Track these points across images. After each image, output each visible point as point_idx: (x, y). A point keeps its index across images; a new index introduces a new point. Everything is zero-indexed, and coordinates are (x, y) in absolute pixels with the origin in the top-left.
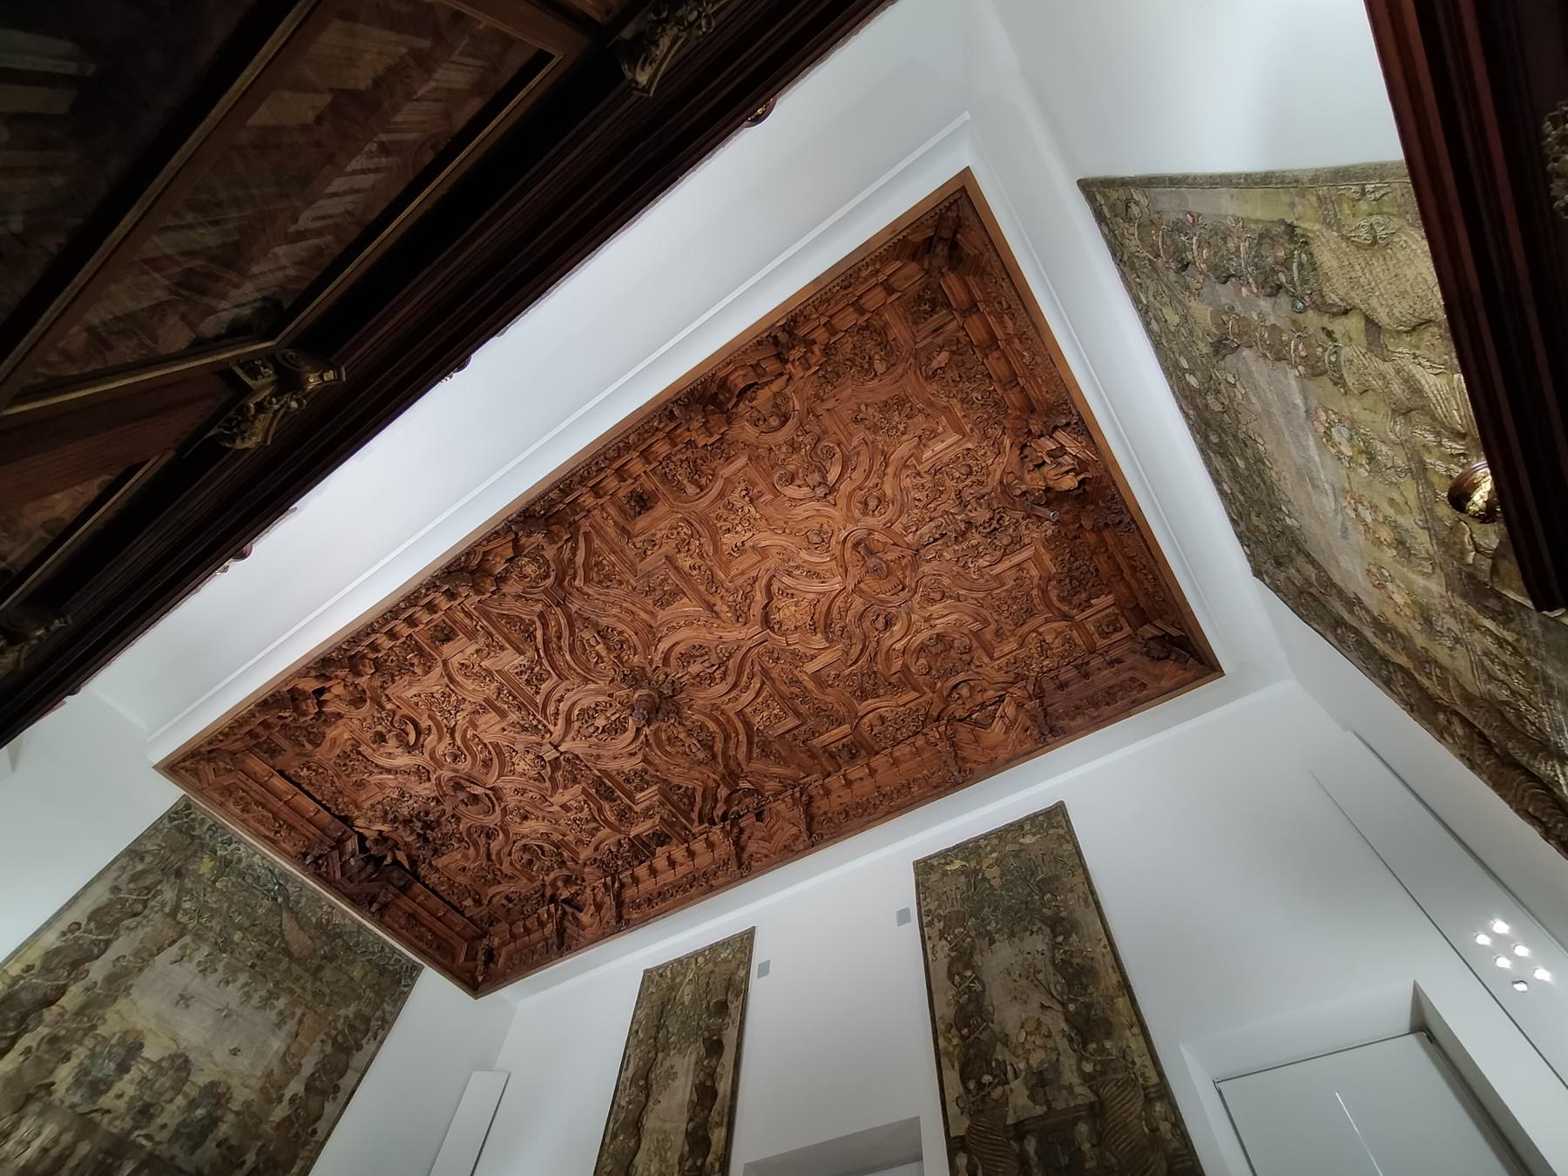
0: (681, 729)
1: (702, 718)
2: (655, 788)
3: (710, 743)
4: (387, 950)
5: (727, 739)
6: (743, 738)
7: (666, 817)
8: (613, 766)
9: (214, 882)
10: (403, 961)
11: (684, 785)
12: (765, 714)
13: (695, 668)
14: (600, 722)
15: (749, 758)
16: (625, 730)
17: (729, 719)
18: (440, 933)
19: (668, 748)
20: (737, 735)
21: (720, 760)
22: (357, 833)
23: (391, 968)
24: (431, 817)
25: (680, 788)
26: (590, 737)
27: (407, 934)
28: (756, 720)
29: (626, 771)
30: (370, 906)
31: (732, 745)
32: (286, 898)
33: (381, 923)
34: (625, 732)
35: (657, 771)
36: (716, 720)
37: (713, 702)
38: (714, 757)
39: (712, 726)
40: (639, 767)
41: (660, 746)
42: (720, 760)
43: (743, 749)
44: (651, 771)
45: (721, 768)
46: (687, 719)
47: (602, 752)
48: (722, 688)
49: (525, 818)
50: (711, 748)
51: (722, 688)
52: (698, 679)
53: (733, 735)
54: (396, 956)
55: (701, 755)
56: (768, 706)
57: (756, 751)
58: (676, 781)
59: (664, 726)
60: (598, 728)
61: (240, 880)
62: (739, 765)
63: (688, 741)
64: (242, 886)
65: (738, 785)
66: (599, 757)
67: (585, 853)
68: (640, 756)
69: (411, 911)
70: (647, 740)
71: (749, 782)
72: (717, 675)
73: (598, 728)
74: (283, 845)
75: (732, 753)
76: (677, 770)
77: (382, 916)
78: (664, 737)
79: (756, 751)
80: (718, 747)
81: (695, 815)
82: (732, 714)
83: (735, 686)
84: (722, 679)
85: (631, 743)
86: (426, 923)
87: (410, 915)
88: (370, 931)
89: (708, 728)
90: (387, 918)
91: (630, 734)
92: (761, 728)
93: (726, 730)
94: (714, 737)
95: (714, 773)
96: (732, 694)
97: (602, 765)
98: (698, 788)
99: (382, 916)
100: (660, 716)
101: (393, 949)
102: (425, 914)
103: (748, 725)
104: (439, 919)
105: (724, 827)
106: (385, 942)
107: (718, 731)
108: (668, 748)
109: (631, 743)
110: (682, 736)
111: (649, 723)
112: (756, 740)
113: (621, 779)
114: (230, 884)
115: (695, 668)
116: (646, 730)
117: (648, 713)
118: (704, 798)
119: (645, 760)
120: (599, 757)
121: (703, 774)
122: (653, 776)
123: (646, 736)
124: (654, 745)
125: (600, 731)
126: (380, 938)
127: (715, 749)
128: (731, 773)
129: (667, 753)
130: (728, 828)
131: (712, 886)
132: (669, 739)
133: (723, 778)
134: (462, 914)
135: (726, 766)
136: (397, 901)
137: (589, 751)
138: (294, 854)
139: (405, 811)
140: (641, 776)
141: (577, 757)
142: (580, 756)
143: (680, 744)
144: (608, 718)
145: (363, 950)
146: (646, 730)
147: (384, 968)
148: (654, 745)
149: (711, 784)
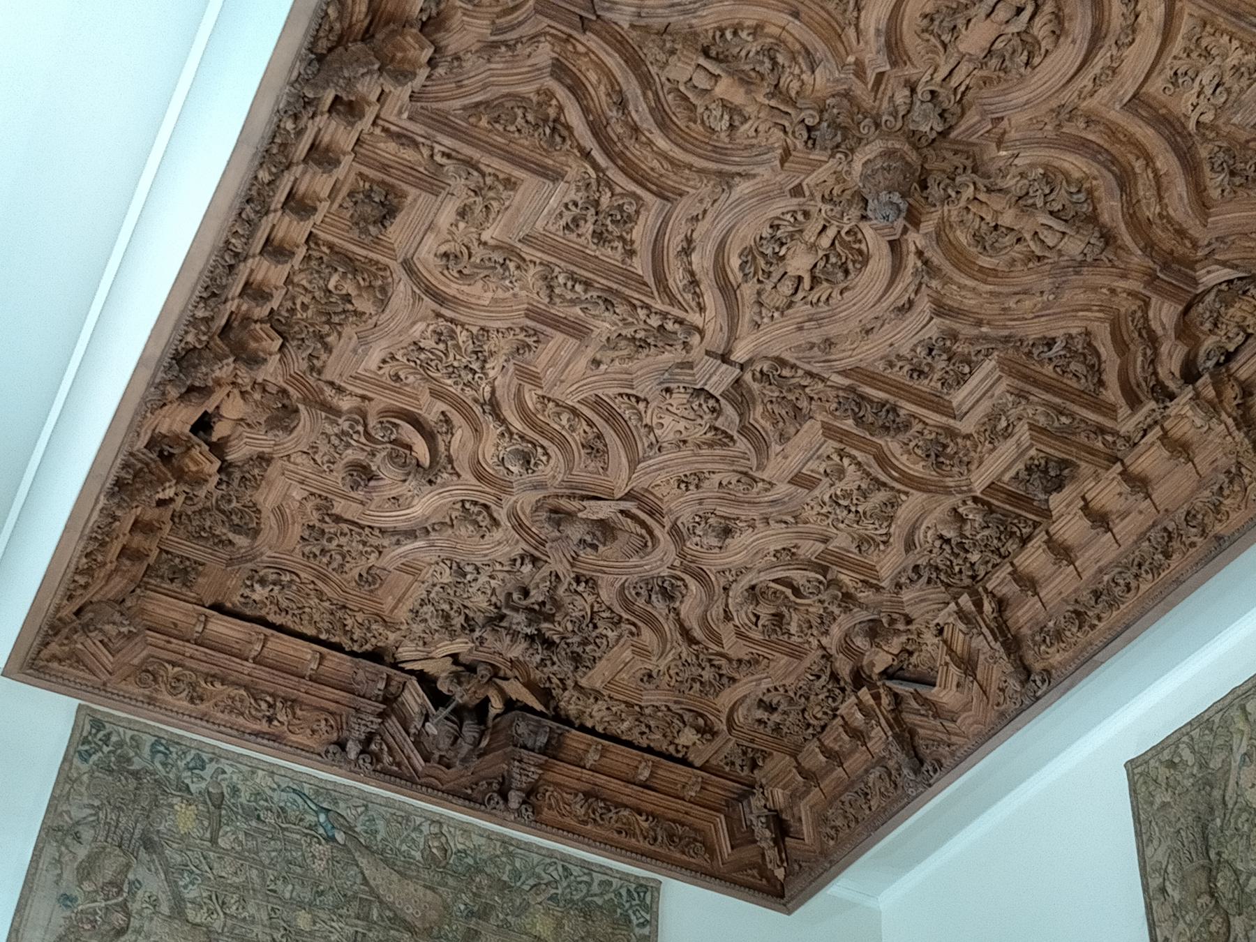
0: (997, 202)
1: (1044, 155)
2: (989, 365)
3: (1086, 208)
4: (576, 871)
5: (1125, 181)
6: (1166, 162)
7: (1042, 421)
8: (869, 353)
9: (213, 841)
10: (616, 883)
11: (1059, 333)
12: (1206, 76)
13: (975, 38)
14: (799, 263)
15: (1202, 204)
16: (864, 258)
17: (1112, 131)
18: (659, 811)
19: (985, 261)
20: (1149, 160)
21: (1126, 238)
22: (411, 672)
23: (599, 901)
24: (536, 596)
25: (1050, 343)
26: (790, 305)
27: (598, 830)
28: (1185, 103)
29: (905, 351)
30: (505, 799)
31: (1144, 188)
32: (349, 830)
33: (539, 823)
34: (865, 263)
35: (979, 323)
36: (1081, 146)
37: (1054, 104)
38: (1108, 238)
39: (1075, 164)
40: (933, 331)
41: (961, 261)
42: (1126, 238)
43: (1179, 188)
44: (966, 330)
45: (1137, 259)
46: (1002, 171)
47: (832, 330)
48: (1067, 55)
49: (727, 532)
50: (1093, 219)
51: (1067, 55)
52: (994, 62)
53: (1138, 165)
54: (598, 877)
55: (1074, 246)
56: (1207, 54)
57: (1215, 182)
58: (1034, 331)
59: (953, 212)
60: (800, 279)
61: (254, 823)
62: (1181, 233)
63: (1026, 226)
64: (264, 833)
65: (1195, 282)
66: (829, 343)
67: (889, 563)
68: (924, 305)
69: (587, 787)
70: (926, 263)
71: (1224, 264)
72: (1041, 29)
73: (800, 279)
74: (293, 738)
75: (1150, 210)
76: (1028, 304)
77: (536, 811)
78: (963, 237)
79: (1215, 182)
80: (1111, 209)
81: (1113, 393)
82: (1115, 114)
83: (1096, 38)
84: (1057, 35)
85: (891, 282)
86: (625, 799)
87: (587, 795)
88: (528, 847)
89: (1067, 175)
90: (547, 814)
91: (881, 262)
92: (1208, 118)
93: (1114, 160)
94: (1090, 192)
95: (1124, 276)
96: (1100, 61)
97: (846, 356)
98: (1094, 326)
99: (536, 811)
100: (935, 192)
101: (584, 864)
102: (615, 784)
103: (1168, 124)
104: (645, 785)
105: (1197, 396)
106: (565, 858)
107: (1094, 169)
108: (985, 261)
109: (891, 282)
110: (1007, 219)
111: (913, 219)
112: (1203, 153)
113: (900, 374)
114: (241, 837)
115: (975, 38)
116: (915, 240)
117: (903, 196)
118: (1121, 346)
119: (941, 309)
120: (829, 343)
121: (1095, 289)
122: (972, 341)
123: (920, 253)
124: (947, 268)
125: (807, 283)
126: (551, 854)
127: (1105, 218)
128: (1169, 261)
129: (986, 274)
130: (1210, 393)
131: (1218, 538)
132: (978, 239)
133: (1151, 280)
134: (684, 762)
135: (1149, 247)
136: (549, 776)
137: (802, 338)
138: (322, 750)
139: (481, 601)
140: (946, 350)
141: (782, 362)
142: (787, 356)
143: (1008, 240)
144: (813, 247)
145: (532, 882)
146: (915, 240)
147: (588, 904)
148: (947, 268)
149: (1126, 305)
